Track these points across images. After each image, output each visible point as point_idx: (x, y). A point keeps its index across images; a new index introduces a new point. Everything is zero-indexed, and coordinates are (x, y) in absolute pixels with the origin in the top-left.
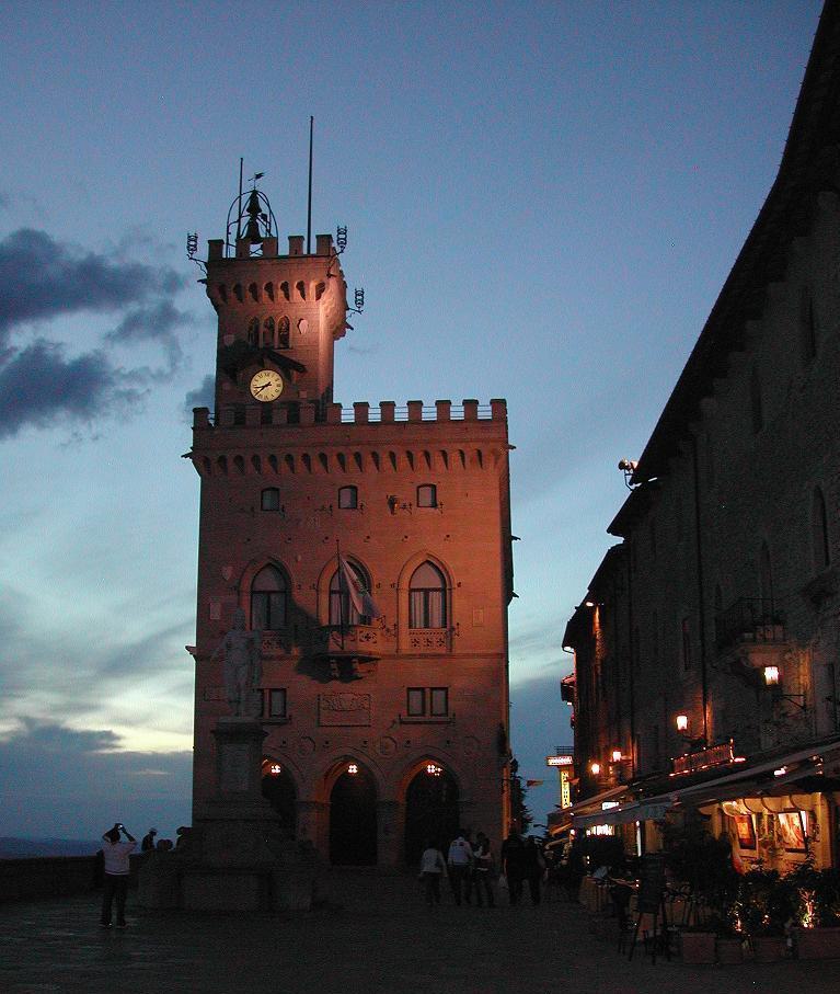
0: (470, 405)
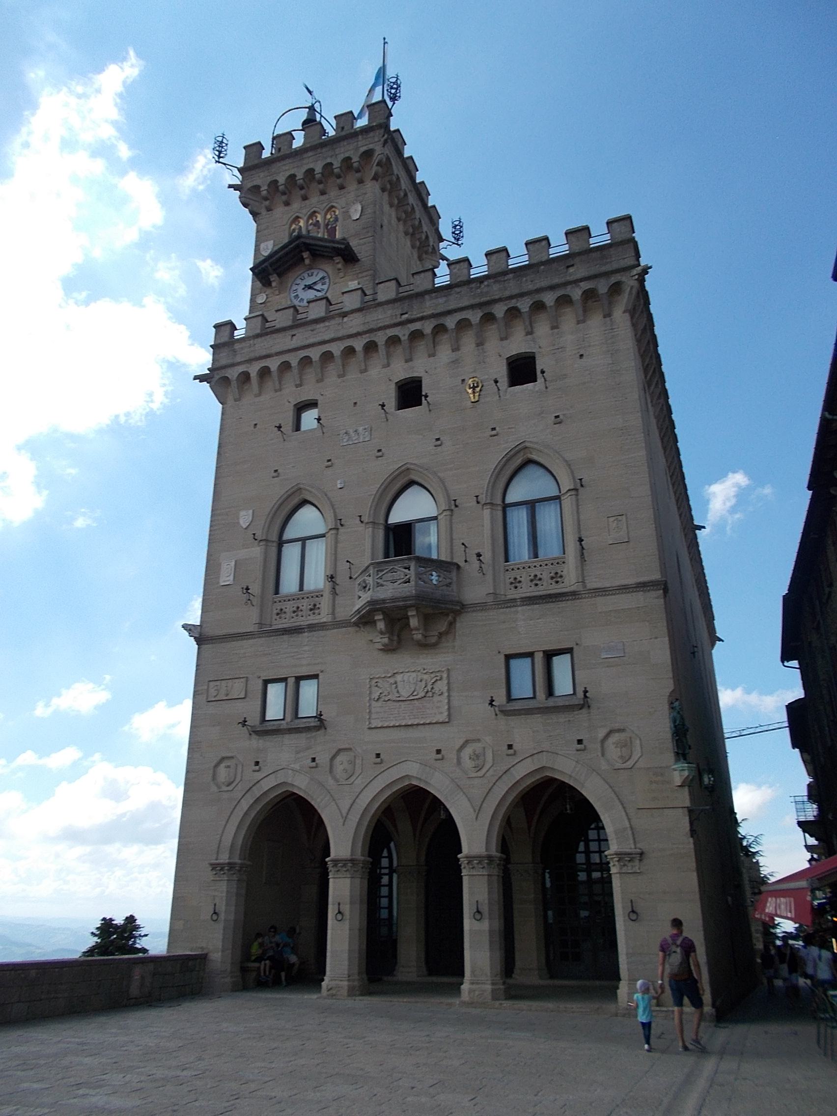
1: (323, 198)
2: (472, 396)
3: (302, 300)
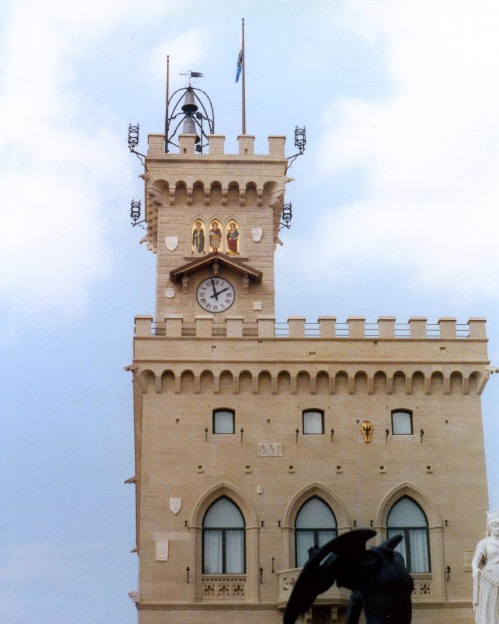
0: (448, 322)
1: (224, 208)
2: (365, 436)
3: (209, 305)
